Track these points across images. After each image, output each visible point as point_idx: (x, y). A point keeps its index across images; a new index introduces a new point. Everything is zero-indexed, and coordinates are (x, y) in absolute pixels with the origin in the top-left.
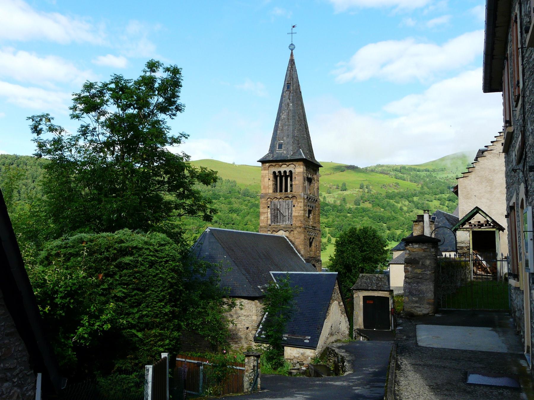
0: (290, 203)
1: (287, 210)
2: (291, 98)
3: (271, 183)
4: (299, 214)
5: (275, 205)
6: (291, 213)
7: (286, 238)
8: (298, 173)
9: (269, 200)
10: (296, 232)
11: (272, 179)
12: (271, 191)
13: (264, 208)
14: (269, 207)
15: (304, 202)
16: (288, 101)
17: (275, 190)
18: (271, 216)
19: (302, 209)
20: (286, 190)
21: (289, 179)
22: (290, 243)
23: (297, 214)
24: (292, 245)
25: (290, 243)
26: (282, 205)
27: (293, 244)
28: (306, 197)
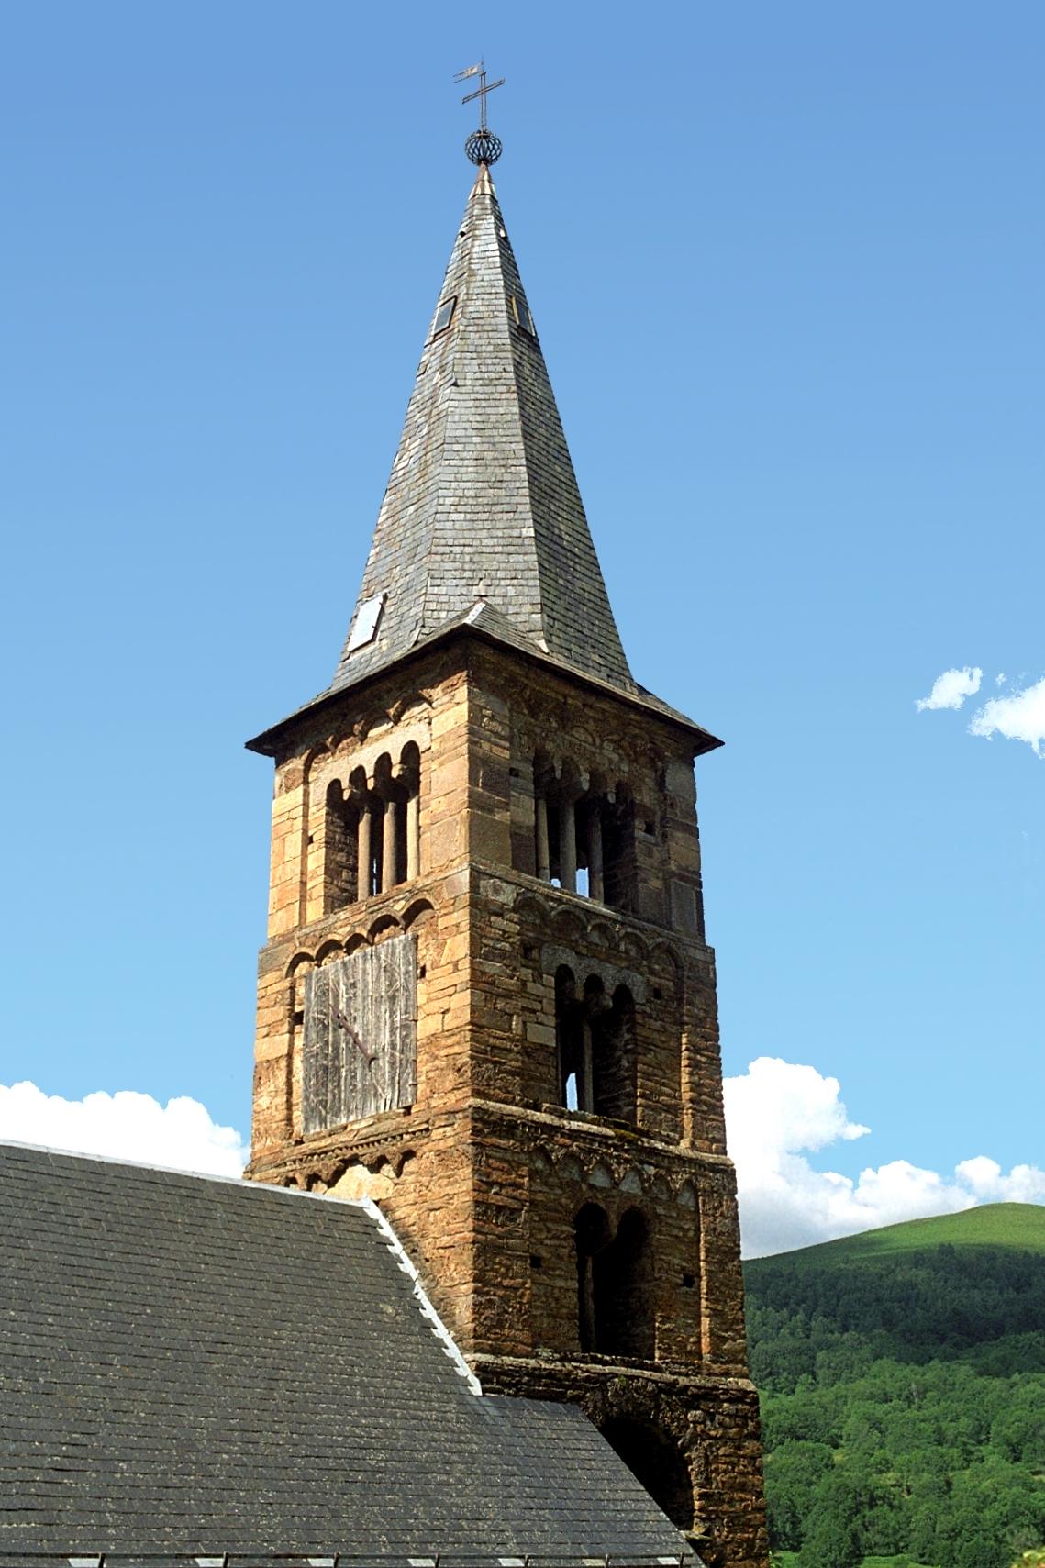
1: (384, 1007)
4: (450, 1022)
7: (374, 1213)
9: (303, 967)
10: (427, 1152)
13: (271, 1029)
14: (297, 1018)
19: (464, 975)
22: (397, 1248)
25: (397, 1248)
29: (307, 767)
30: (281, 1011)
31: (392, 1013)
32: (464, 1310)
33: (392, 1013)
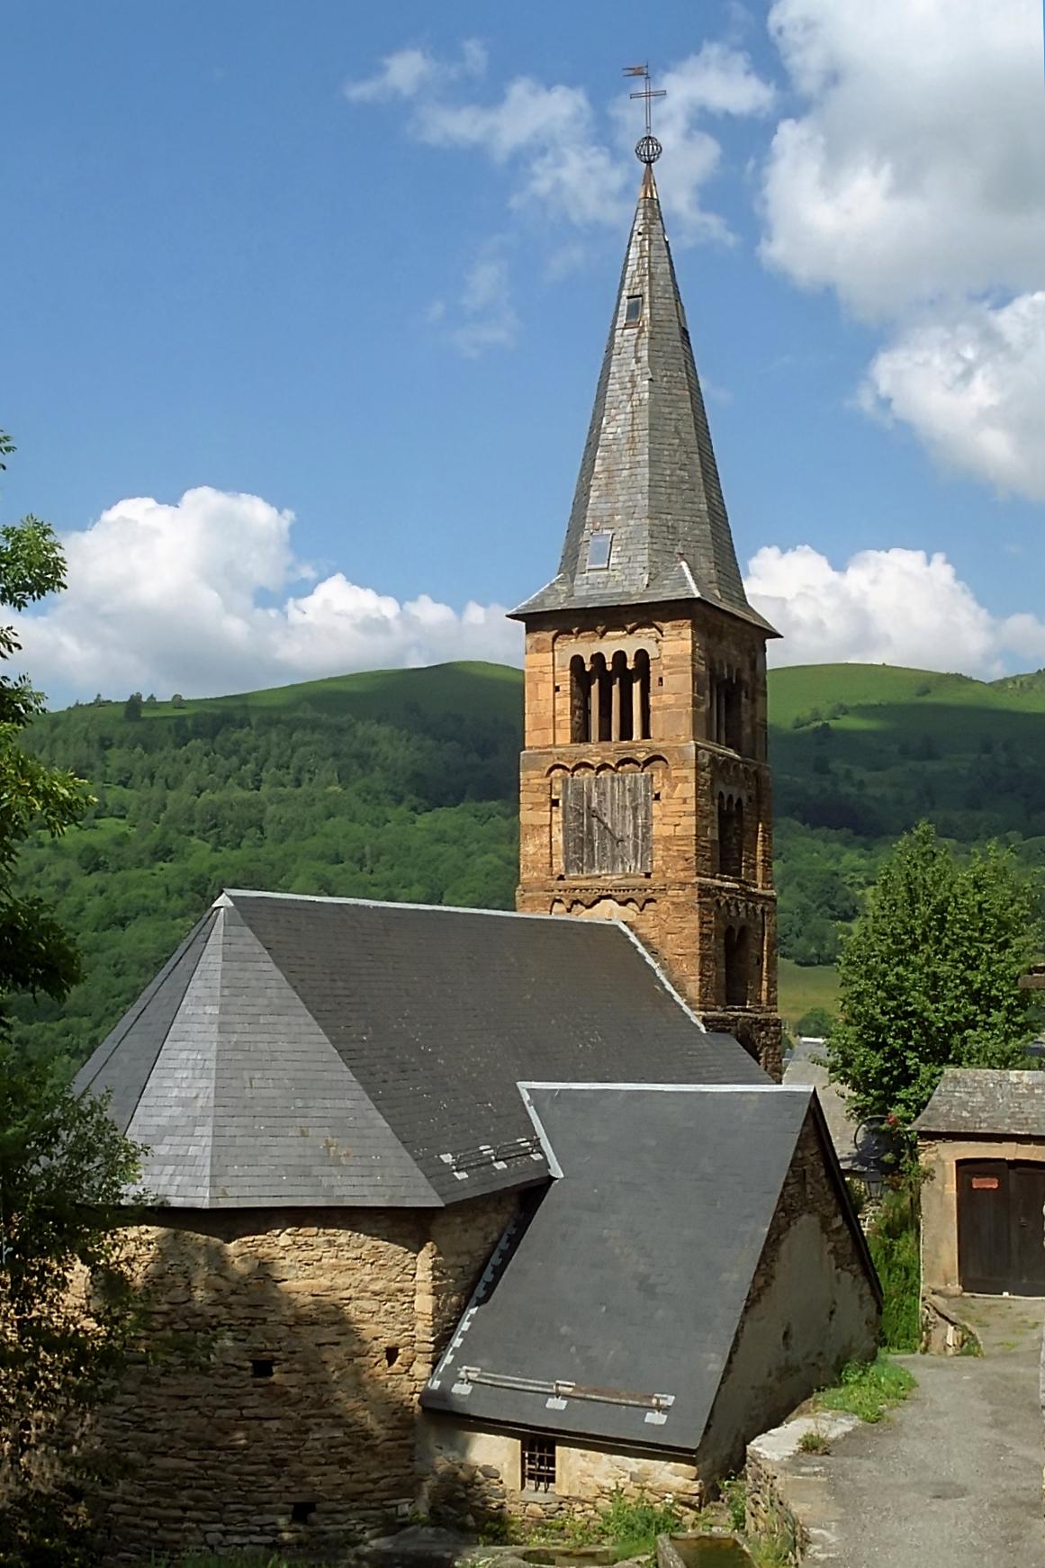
0: (641, 784)
1: (629, 813)
2: (644, 354)
3: (564, 703)
5: (579, 794)
6: (647, 827)
7: (625, 929)
8: (672, 658)
10: (664, 904)
11: (566, 687)
12: (564, 736)
13: (536, 806)
14: (555, 803)
15: (697, 781)
16: (633, 366)
17: (581, 734)
18: (566, 842)
19: (691, 807)
20: (626, 733)
21: (636, 687)
22: (641, 949)
23: (668, 831)
24: (649, 960)
25: (641, 949)
26: (609, 795)
27: (654, 953)
28: (706, 760)
29: (554, 640)
30: (544, 798)
31: (635, 817)
32: (693, 988)
33: (635, 817)
